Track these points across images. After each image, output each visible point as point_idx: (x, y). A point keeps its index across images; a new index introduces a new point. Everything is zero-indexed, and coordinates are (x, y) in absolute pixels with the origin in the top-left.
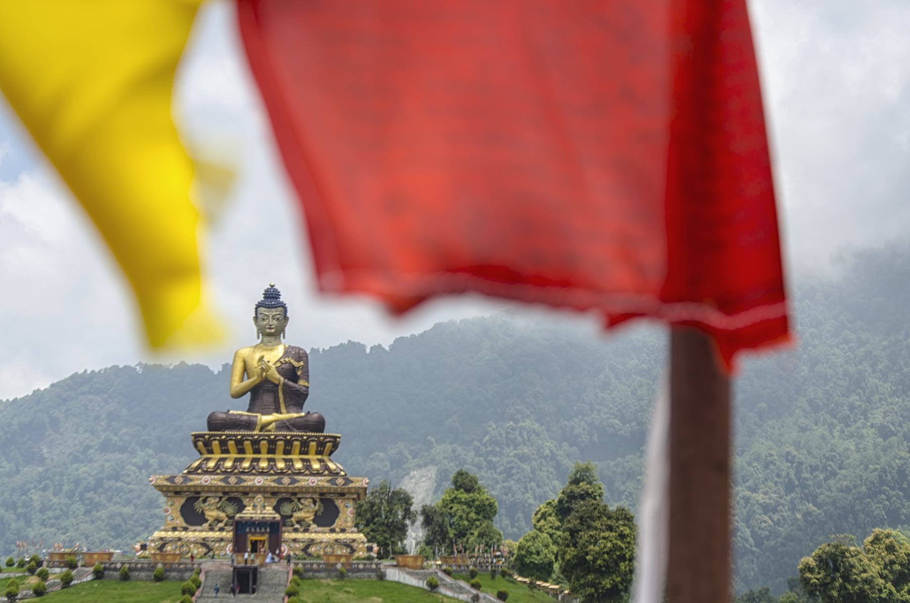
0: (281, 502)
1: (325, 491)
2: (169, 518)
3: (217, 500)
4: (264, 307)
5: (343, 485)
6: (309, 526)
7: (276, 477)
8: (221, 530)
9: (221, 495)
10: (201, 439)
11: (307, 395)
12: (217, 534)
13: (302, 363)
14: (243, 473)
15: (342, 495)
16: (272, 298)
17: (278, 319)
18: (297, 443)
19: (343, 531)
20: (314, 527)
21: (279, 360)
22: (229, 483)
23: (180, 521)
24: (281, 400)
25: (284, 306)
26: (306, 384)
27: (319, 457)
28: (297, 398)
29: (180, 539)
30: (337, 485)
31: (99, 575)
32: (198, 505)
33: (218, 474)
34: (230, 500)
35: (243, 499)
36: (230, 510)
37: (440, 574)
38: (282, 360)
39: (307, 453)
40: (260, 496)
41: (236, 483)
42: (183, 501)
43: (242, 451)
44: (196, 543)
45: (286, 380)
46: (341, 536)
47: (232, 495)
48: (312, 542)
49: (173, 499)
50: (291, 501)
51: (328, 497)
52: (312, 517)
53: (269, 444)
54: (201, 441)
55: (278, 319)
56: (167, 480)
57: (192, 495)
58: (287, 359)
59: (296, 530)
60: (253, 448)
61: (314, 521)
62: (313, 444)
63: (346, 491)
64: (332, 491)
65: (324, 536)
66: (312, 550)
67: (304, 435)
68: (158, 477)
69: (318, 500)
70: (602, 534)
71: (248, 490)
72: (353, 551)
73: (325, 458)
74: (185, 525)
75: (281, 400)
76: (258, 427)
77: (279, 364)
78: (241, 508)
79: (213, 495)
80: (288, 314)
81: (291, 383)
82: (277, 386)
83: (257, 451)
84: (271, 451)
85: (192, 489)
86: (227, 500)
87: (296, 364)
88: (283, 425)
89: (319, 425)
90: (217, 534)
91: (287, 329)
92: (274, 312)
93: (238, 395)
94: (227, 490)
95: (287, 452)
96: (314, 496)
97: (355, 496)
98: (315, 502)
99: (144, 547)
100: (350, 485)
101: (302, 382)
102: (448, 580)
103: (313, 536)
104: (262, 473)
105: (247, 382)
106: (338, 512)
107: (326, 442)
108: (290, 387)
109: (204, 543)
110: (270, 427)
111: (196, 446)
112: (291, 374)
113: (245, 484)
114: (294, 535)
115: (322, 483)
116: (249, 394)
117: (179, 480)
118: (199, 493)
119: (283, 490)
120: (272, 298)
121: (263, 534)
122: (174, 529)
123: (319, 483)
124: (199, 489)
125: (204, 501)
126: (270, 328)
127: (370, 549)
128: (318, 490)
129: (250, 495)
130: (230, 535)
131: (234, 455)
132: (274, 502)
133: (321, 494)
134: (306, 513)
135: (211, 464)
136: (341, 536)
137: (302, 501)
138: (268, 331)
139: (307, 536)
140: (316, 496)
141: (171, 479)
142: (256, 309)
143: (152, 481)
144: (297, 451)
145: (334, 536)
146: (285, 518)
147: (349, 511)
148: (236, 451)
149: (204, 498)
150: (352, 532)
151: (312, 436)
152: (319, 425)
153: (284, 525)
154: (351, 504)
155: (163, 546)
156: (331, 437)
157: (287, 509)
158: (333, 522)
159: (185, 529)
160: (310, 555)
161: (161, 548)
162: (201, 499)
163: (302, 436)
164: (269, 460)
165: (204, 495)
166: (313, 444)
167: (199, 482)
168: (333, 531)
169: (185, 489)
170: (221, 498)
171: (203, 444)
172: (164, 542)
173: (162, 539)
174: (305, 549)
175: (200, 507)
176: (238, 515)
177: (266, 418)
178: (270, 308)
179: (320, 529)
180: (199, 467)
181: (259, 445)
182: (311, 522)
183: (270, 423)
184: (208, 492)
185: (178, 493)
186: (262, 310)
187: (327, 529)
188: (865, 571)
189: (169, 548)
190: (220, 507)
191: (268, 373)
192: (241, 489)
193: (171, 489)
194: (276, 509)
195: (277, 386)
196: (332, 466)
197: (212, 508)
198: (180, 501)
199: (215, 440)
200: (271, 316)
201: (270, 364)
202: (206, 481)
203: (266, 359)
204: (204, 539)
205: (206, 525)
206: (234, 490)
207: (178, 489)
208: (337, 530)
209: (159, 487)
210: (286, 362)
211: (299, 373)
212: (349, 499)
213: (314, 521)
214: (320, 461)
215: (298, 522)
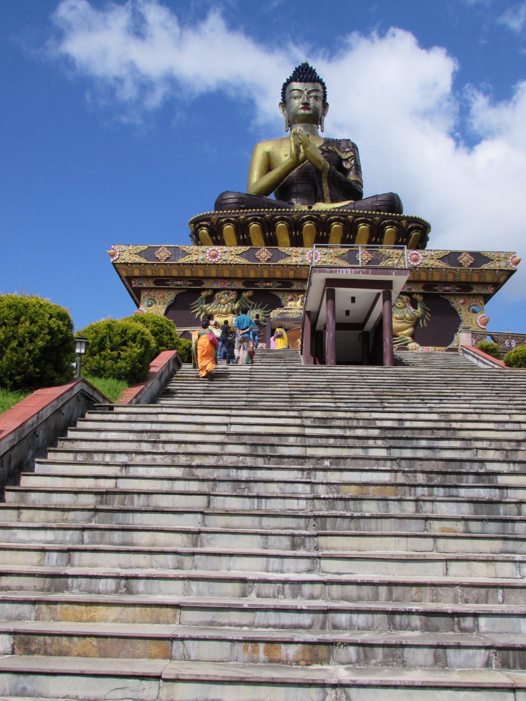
1: (436, 278)
3: (233, 296)
4: (296, 81)
5: (471, 265)
6: (406, 344)
9: (239, 285)
10: (205, 223)
22: (258, 260)
25: (323, 84)
26: (359, 180)
30: (461, 265)
35: (280, 296)
38: (324, 148)
41: (269, 260)
42: (170, 297)
45: (333, 168)
47: (261, 286)
49: (152, 293)
51: (440, 290)
52: (410, 330)
53: (318, 229)
54: (206, 226)
55: (316, 98)
56: (140, 254)
57: (186, 285)
58: (330, 148)
60: (291, 236)
61: (413, 336)
63: (476, 279)
64: (450, 278)
67: (375, 215)
68: (124, 247)
69: (419, 298)
71: (291, 274)
80: (328, 101)
82: (319, 172)
85: (188, 273)
86: (250, 298)
87: (344, 156)
94: (252, 275)
96: (414, 291)
97: (490, 290)
100: (485, 267)
101: (352, 177)
106: (460, 321)
107: (412, 229)
113: (288, 261)
115: (431, 262)
117: (162, 255)
118: (198, 280)
123: (426, 262)
124: (201, 274)
126: (309, 109)
128: (423, 277)
129: (296, 286)
133: (429, 285)
138: (303, 111)
141: (148, 253)
143: (113, 256)
147: (479, 318)
148: (263, 243)
149: (210, 293)
151: (388, 217)
158: (451, 340)
162: (204, 294)
163: (372, 216)
167: (201, 257)
169: (175, 273)
170: (239, 292)
175: (202, 310)
178: (305, 81)
181: (301, 229)
182: (409, 338)
190: (238, 310)
191: (308, 149)
193: (149, 273)
197: (224, 310)
199: (228, 221)
200: (306, 92)
202: (215, 256)
206: (266, 275)
207: (162, 273)
210: (329, 151)
212: (475, 296)
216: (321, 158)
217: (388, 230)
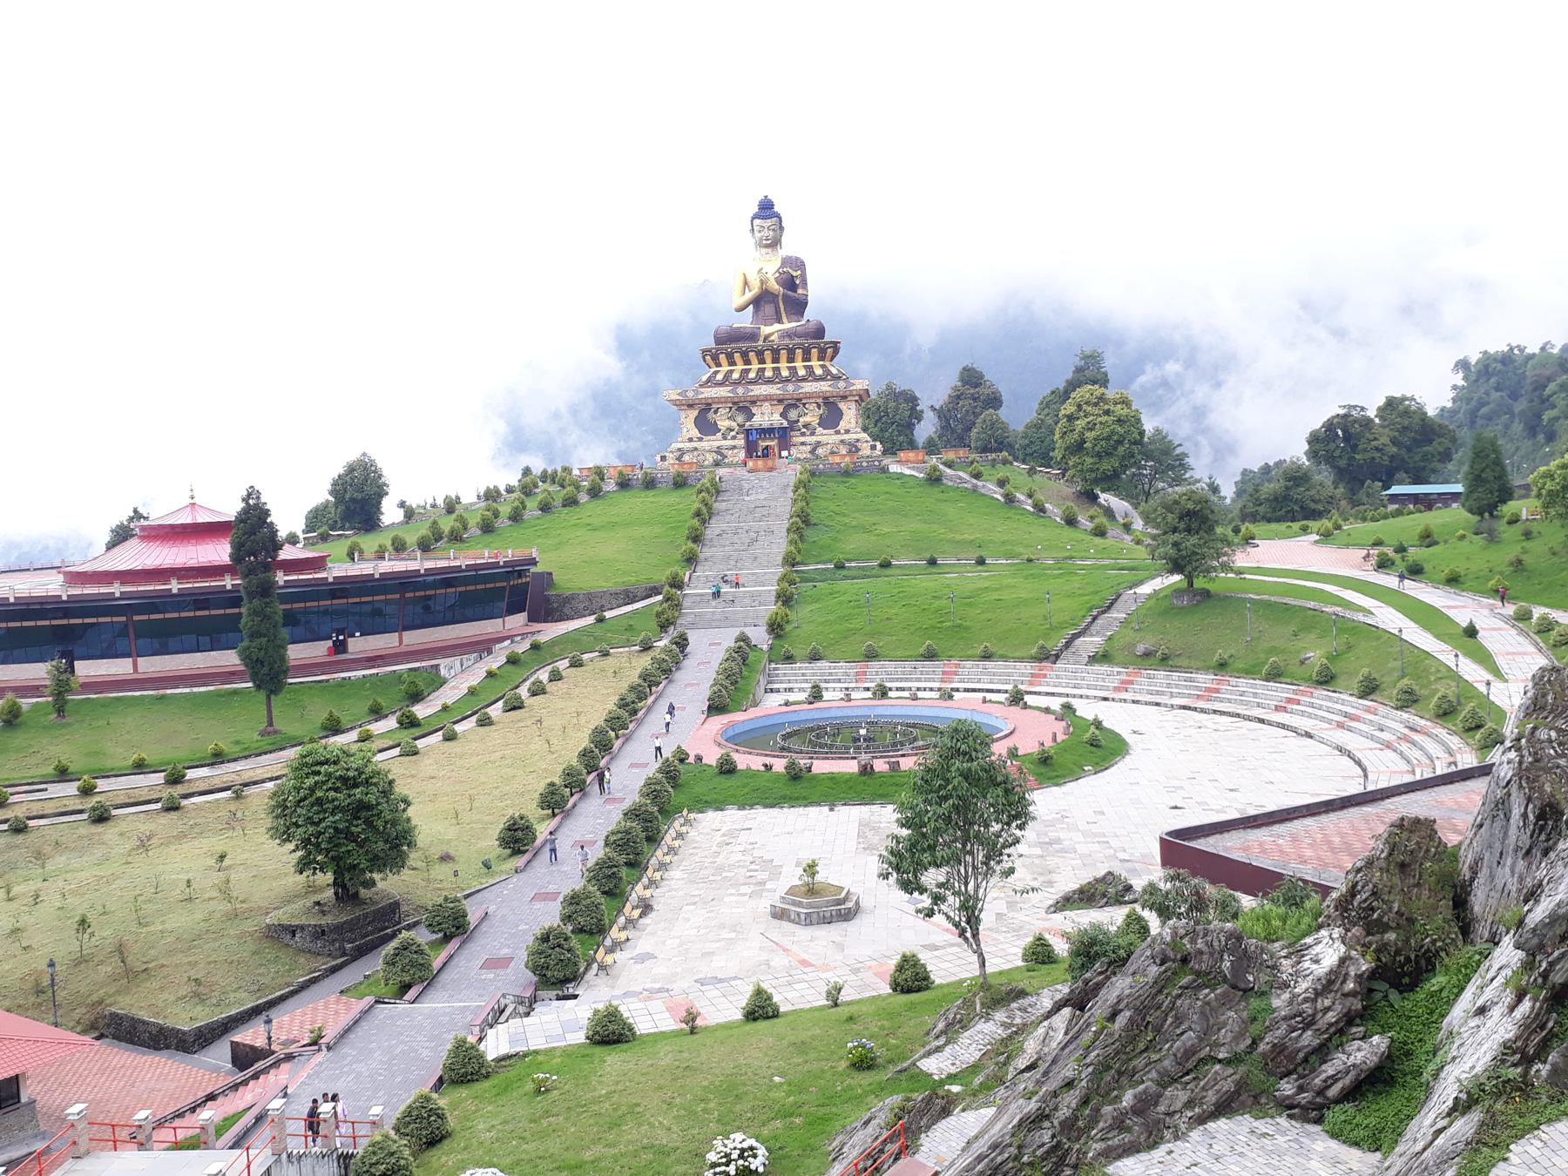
0: (788, 408)
1: (828, 394)
2: (685, 430)
3: (728, 410)
7: (780, 385)
8: (734, 438)
11: (807, 303)
12: (729, 443)
13: (799, 272)
14: (750, 383)
15: (844, 398)
16: (766, 209)
17: (774, 230)
18: (799, 352)
19: (847, 432)
20: (819, 430)
21: (778, 271)
23: (695, 433)
24: (782, 310)
25: (778, 216)
27: (821, 363)
28: (798, 306)
29: (696, 449)
31: (624, 484)
32: (711, 415)
33: (727, 386)
34: (739, 409)
36: (740, 419)
37: (941, 466)
39: (810, 361)
40: (767, 404)
42: (696, 413)
43: (747, 362)
44: (710, 451)
46: (846, 437)
48: (818, 444)
50: (795, 406)
55: (774, 230)
59: (803, 434)
61: (819, 424)
62: (814, 351)
65: (828, 437)
66: (820, 451)
70: (1099, 419)
72: (858, 450)
73: (827, 364)
74: (699, 435)
75: (782, 310)
76: (762, 339)
77: (777, 275)
78: (750, 416)
79: (724, 405)
80: (783, 224)
81: (790, 293)
82: (777, 296)
83: (762, 361)
84: (776, 360)
85: (703, 401)
87: (794, 274)
88: (789, 334)
89: (819, 332)
90: (729, 443)
91: (784, 239)
92: (769, 222)
93: (741, 309)
94: (736, 400)
95: (791, 359)
97: (857, 398)
98: (819, 407)
99: (663, 458)
101: (800, 291)
102: (948, 471)
103: (819, 438)
104: (769, 381)
105: (749, 295)
108: (789, 297)
109: (719, 451)
110: (772, 338)
111: (705, 361)
112: (790, 283)
113: (752, 394)
114: (802, 439)
116: (751, 306)
117: (690, 394)
118: (710, 404)
119: (788, 397)
120: (766, 209)
121: (772, 440)
122: (691, 440)
124: (710, 401)
125: (716, 412)
127: (873, 448)
130: (742, 442)
131: (740, 367)
132: (781, 408)
133: (825, 398)
134: (812, 416)
135: (720, 377)
136: (846, 437)
137: (807, 406)
139: (813, 439)
140: (820, 401)
142: (752, 221)
144: (800, 358)
145: (840, 437)
146: (793, 424)
150: (856, 433)
152: (819, 332)
153: (792, 430)
154: (853, 405)
155: (681, 456)
156: (831, 342)
157: (793, 414)
159: (700, 439)
160: (818, 457)
161: (679, 459)
164: (774, 369)
165: (715, 406)
166: (814, 351)
168: (838, 433)
169: (697, 402)
171: (712, 357)
172: (682, 452)
173: (679, 450)
174: (813, 452)
176: (748, 423)
177: (766, 330)
179: (825, 432)
180: (709, 380)
183: (772, 334)
184: (718, 403)
185: (691, 406)
186: (757, 222)
187: (832, 431)
188: (1375, 439)
189: (686, 458)
192: (749, 399)
194: (783, 415)
195: (777, 296)
196: (834, 371)
198: (694, 413)
201: (769, 275)
203: (764, 271)
204: (718, 447)
205: (719, 435)
206: (742, 399)
207: (691, 402)
208: (842, 431)
209: (674, 402)
211: (798, 282)
213: (819, 424)
214: (822, 366)
215: (804, 426)
216: (777, 287)
217: (813, 350)
